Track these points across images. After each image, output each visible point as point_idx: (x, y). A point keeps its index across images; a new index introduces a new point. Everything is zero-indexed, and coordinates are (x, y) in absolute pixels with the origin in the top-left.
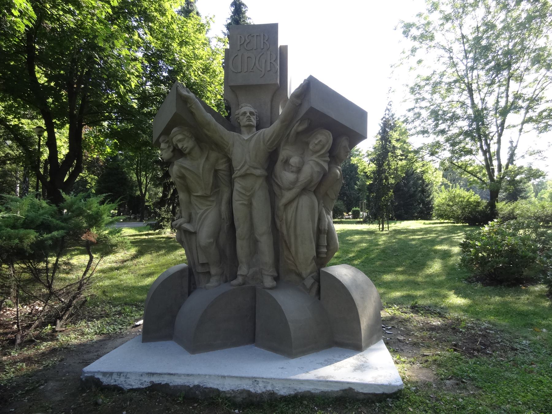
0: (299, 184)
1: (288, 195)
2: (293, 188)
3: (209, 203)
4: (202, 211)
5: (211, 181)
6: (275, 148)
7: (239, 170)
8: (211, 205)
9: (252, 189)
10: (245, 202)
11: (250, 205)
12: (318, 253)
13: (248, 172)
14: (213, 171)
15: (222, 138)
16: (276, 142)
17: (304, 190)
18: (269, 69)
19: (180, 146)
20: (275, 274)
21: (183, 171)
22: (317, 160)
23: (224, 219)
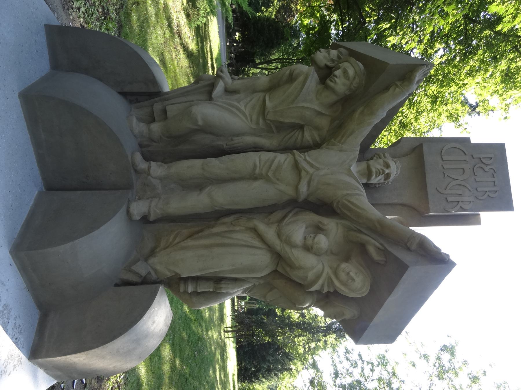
0: (287, 249)
1: (270, 233)
2: (281, 241)
3: (254, 117)
4: (243, 108)
5: (287, 121)
6: (339, 211)
7: (305, 160)
8: (251, 121)
9: (278, 179)
10: (257, 171)
11: (254, 177)
12: (186, 280)
13: (303, 173)
14: (301, 122)
15: (351, 134)
16: (348, 213)
17: (279, 257)
18: (450, 199)
19: (338, 73)
20: (152, 218)
21: (301, 78)
22: (324, 275)
23: (232, 140)
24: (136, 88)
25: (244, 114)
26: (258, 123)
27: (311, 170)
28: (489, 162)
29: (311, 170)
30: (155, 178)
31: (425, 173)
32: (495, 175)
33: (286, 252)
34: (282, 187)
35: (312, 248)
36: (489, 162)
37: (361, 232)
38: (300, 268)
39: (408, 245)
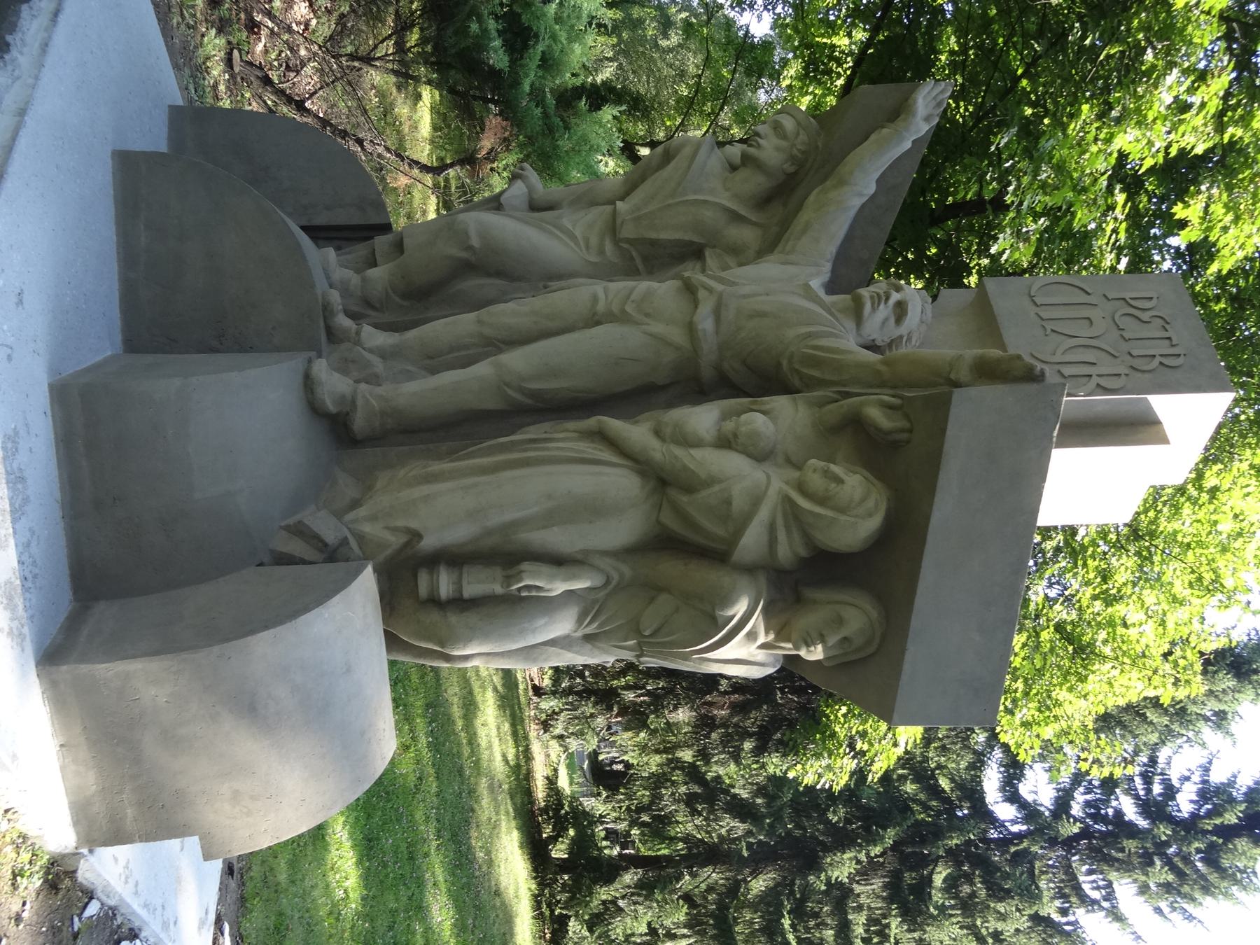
0: (679, 452)
3: (594, 241)
5: (664, 235)
8: (588, 247)
9: (647, 315)
10: (601, 307)
11: (594, 320)
12: (435, 560)
13: (702, 294)
14: (696, 239)
15: (804, 231)
16: (815, 373)
20: (359, 423)
21: (687, 151)
22: (772, 492)
24: (342, 217)
25: (573, 237)
26: (601, 252)
27: (719, 287)
28: (1148, 305)
29: (719, 287)
30: (371, 351)
31: (998, 329)
32: (1167, 327)
33: (676, 457)
34: (658, 328)
35: (735, 435)
36: (1148, 305)
37: (848, 395)
38: (711, 481)
39: (953, 376)
